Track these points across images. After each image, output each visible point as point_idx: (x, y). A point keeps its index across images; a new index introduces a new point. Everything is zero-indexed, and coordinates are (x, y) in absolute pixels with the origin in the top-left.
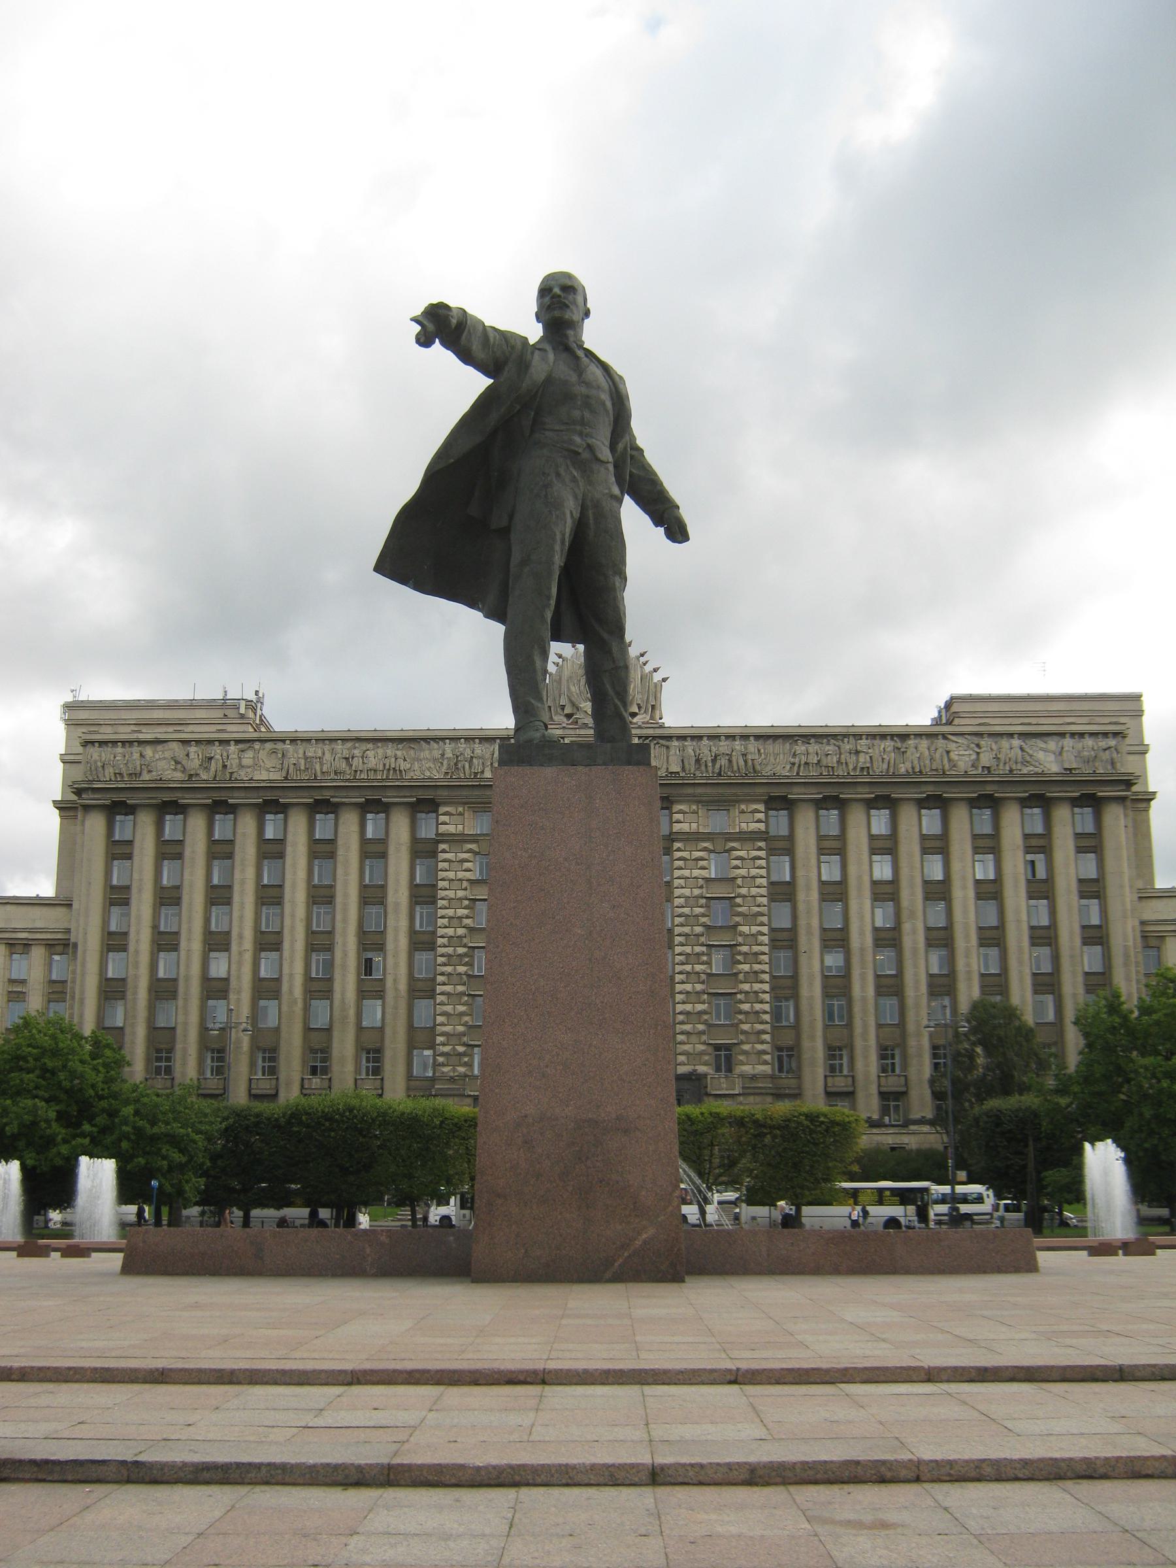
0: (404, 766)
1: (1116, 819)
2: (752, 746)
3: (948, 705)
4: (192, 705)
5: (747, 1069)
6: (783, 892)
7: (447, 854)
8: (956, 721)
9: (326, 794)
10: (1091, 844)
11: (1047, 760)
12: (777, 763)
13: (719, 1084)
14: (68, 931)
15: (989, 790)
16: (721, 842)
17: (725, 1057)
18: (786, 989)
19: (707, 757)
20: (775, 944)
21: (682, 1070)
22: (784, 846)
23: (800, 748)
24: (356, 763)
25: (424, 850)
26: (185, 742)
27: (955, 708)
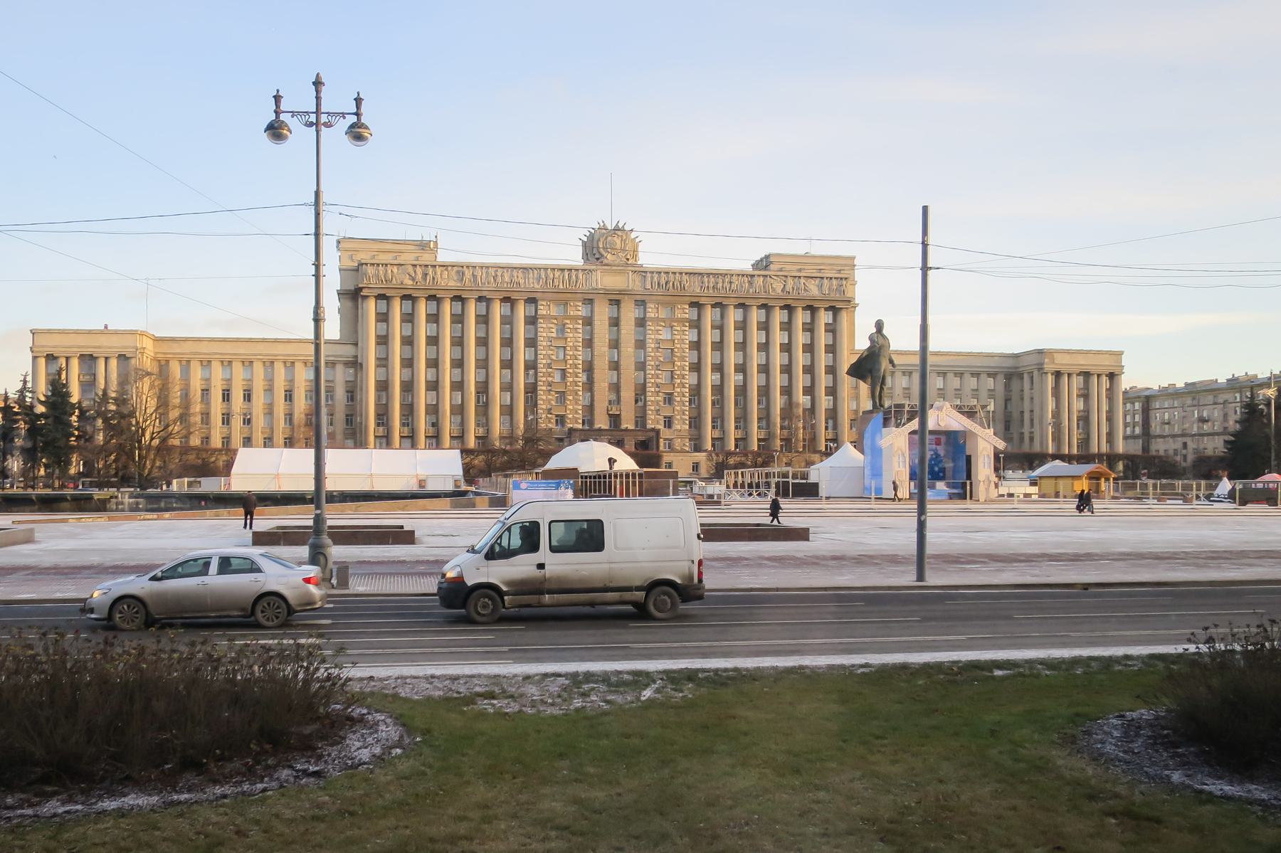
0: (522, 281)
1: (844, 316)
2: (685, 277)
3: (767, 257)
4: (405, 242)
5: (679, 427)
6: (697, 346)
7: (542, 324)
8: (772, 267)
9: (484, 294)
10: (832, 329)
11: (813, 290)
12: (694, 287)
13: (665, 433)
14: (356, 357)
15: (789, 302)
16: (670, 323)
17: (669, 423)
18: (696, 391)
19: (663, 282)
20: (691, 370)
21: (649, 426)
22: (696, 325)
23: (706, 279)
24: (499, 279)
25: (532, 321)
26: (415, 266)
27: (772, 259)
